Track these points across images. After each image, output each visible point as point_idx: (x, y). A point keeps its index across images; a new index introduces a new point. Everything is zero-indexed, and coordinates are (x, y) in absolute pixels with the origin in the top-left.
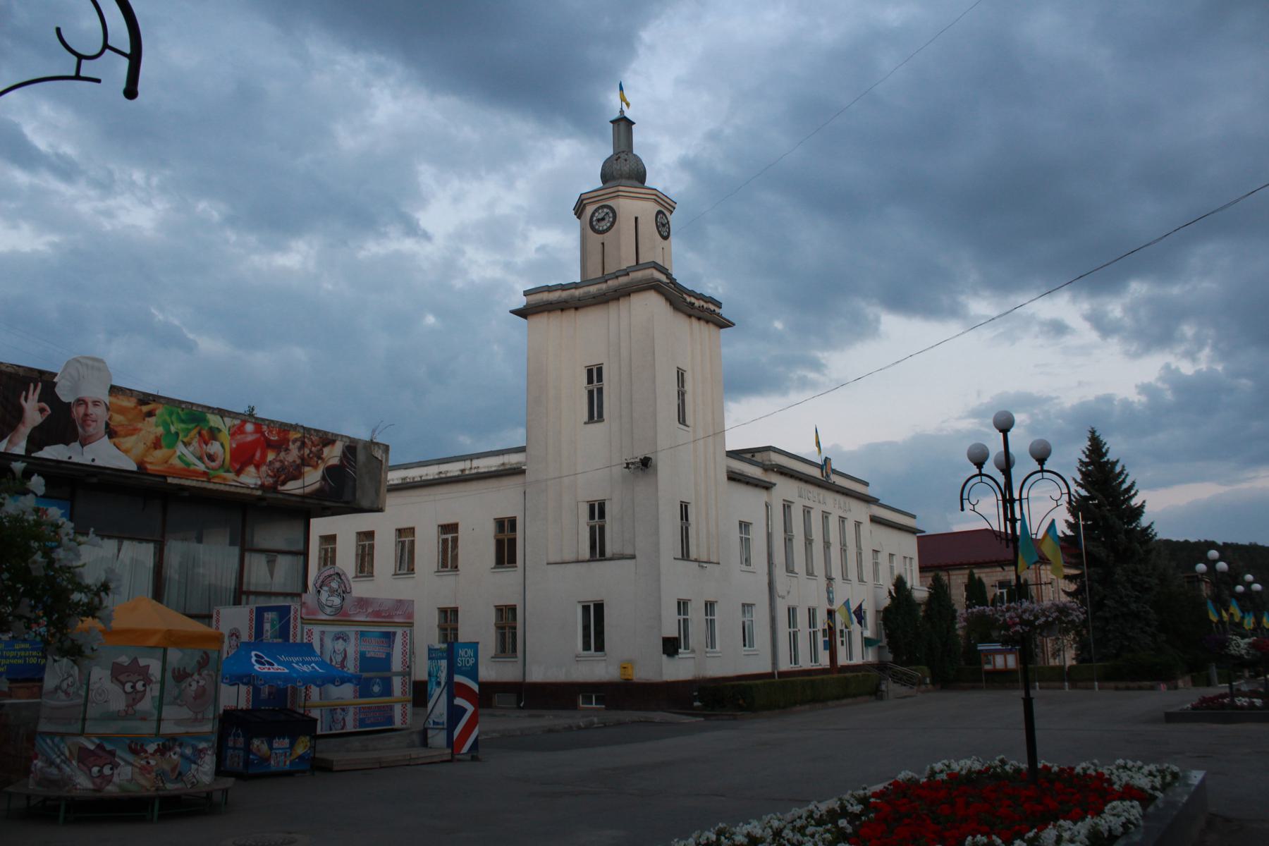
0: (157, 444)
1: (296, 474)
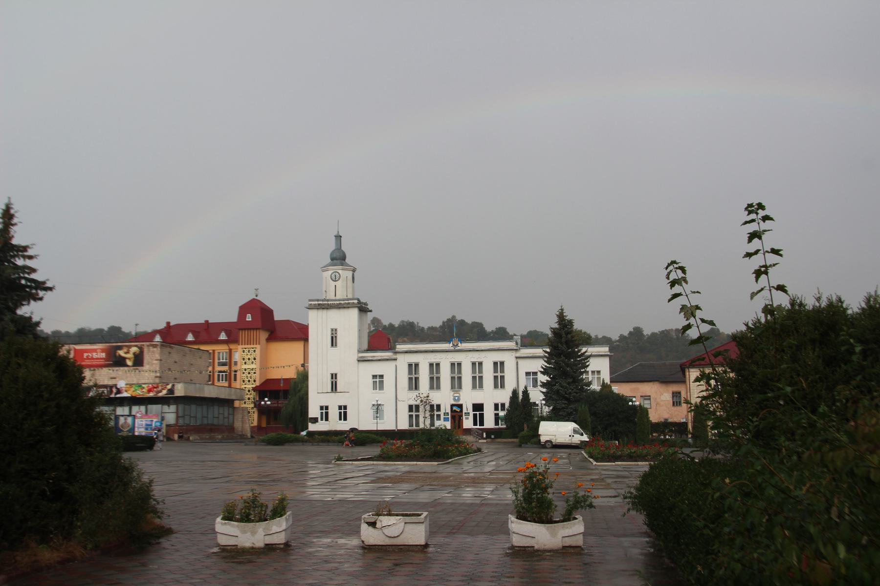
0: (134, 391)
1: (160, 391)
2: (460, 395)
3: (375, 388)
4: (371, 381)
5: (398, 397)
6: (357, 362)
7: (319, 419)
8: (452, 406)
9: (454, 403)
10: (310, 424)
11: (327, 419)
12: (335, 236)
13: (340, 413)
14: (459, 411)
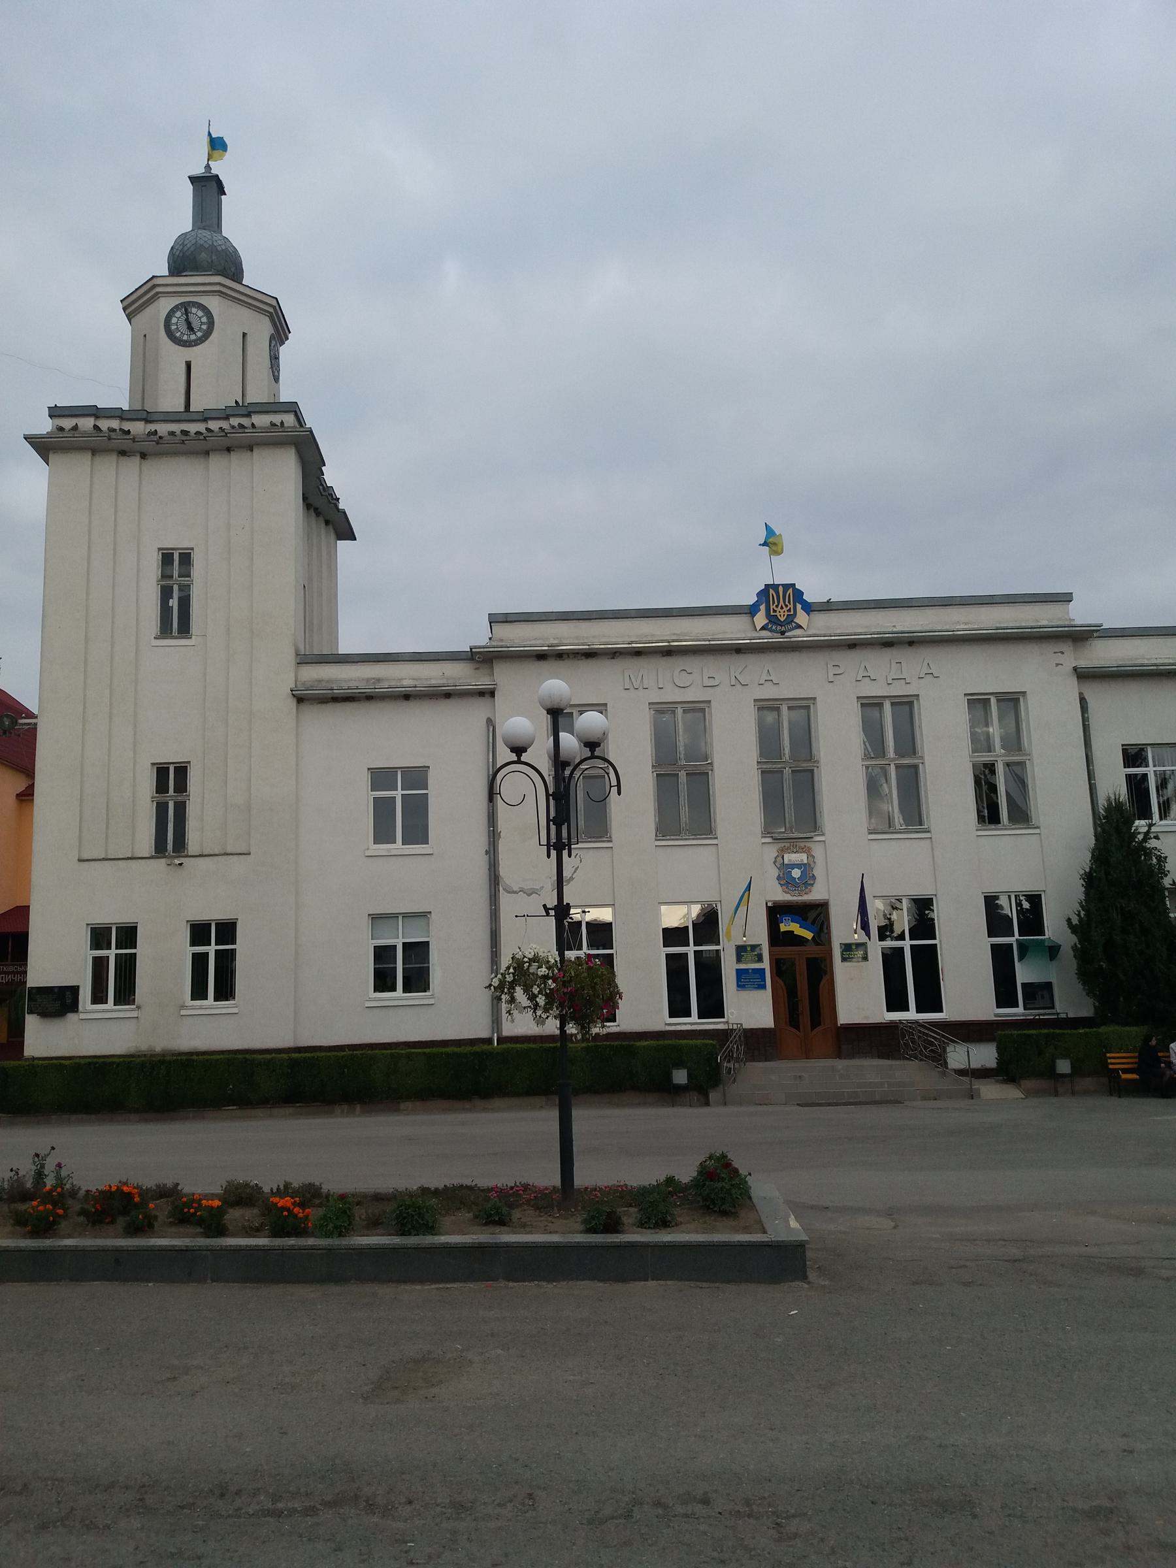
2: (810, 856)
3: (383, 833)
4: (363, 798)
5: (503, 872)
6: (292, 703)
7: (85, 994)
8: (775, 912)
9: (780, 895)
10: (32, 1023)
11: (126, 993)
12: (193, 179)
13: (199, 962)
14: (808, 935)
